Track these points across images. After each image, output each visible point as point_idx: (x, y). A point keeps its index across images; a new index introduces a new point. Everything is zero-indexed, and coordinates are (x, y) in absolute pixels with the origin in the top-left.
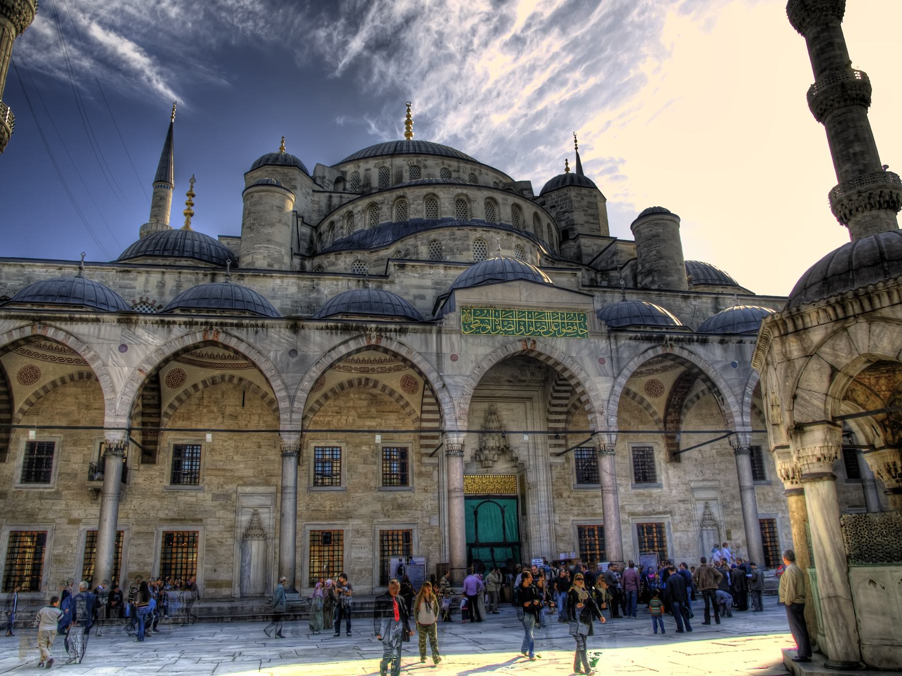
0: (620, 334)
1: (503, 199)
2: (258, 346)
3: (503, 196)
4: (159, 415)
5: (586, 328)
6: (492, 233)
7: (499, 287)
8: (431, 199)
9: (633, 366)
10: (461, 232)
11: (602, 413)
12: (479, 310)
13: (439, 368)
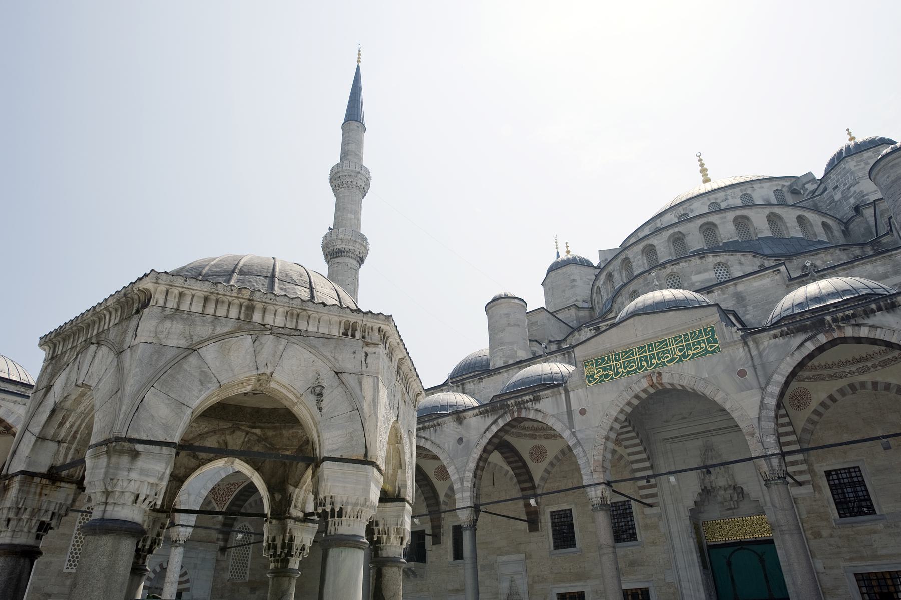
2: (437, 441)
4: (438, 503)
5: (716, 341)
7: (614, 330)
11: (753, 435)
13: (571, 426)
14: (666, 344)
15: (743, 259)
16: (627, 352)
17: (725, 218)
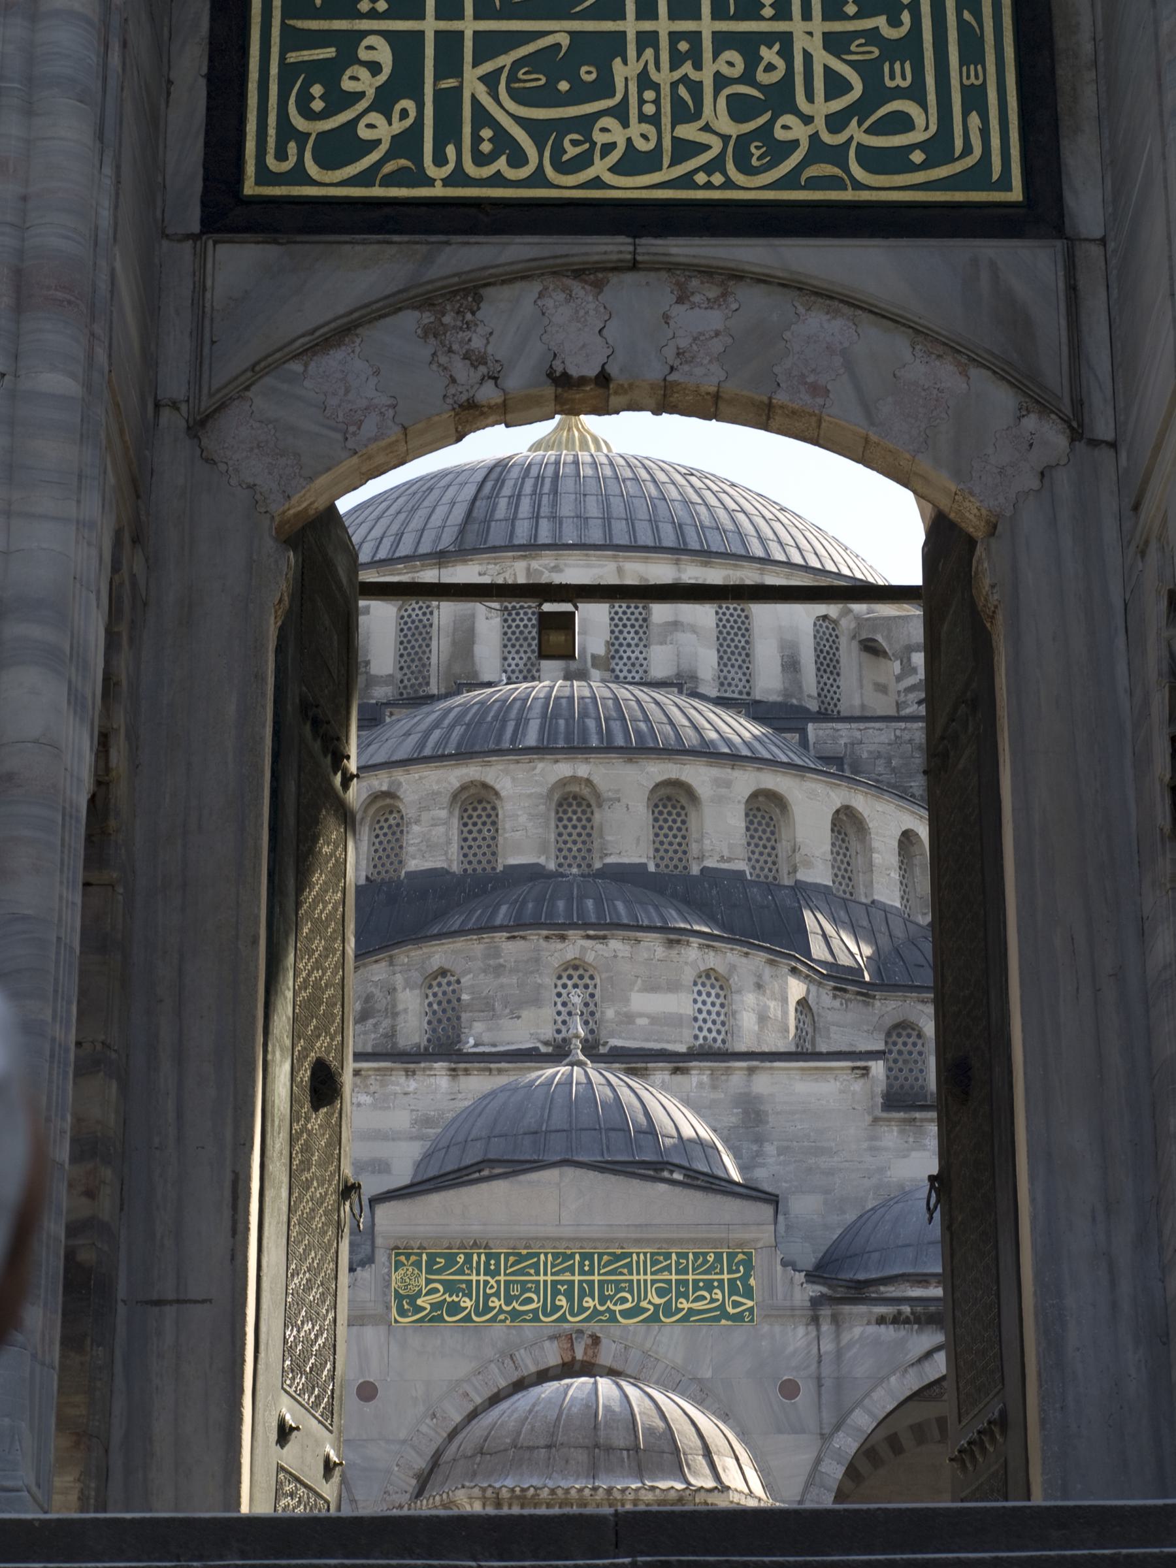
0: (847, 1309)
1: (717, 782)
3: (715, 772)
6: (614, 944)
7: (500, 1187)
8: (477, 803)
9: (884, 1400)
10: (520, 944)
12: (441, 1257)
14: (629, 1266)
15: (767, 971)
16: (521, 1258)
17: (728, 784)
